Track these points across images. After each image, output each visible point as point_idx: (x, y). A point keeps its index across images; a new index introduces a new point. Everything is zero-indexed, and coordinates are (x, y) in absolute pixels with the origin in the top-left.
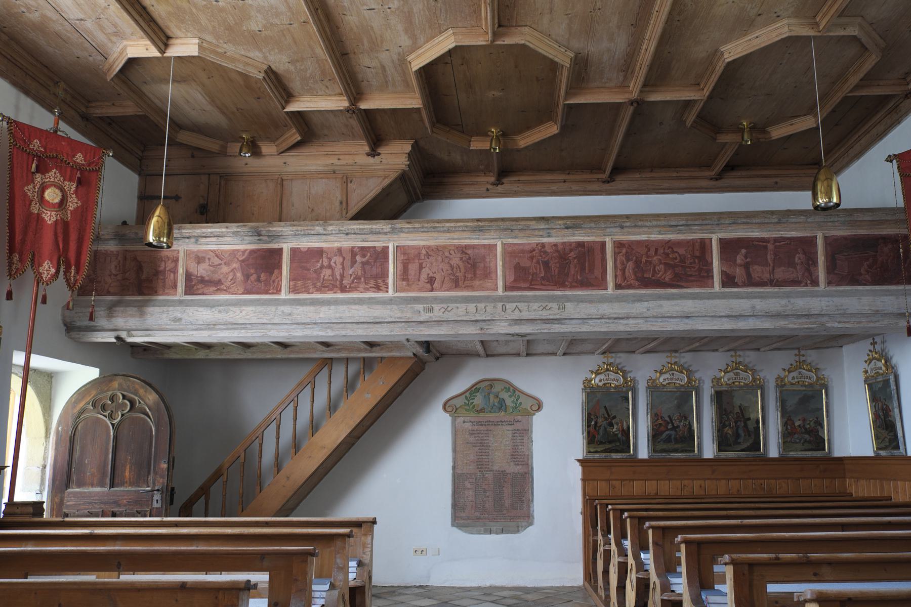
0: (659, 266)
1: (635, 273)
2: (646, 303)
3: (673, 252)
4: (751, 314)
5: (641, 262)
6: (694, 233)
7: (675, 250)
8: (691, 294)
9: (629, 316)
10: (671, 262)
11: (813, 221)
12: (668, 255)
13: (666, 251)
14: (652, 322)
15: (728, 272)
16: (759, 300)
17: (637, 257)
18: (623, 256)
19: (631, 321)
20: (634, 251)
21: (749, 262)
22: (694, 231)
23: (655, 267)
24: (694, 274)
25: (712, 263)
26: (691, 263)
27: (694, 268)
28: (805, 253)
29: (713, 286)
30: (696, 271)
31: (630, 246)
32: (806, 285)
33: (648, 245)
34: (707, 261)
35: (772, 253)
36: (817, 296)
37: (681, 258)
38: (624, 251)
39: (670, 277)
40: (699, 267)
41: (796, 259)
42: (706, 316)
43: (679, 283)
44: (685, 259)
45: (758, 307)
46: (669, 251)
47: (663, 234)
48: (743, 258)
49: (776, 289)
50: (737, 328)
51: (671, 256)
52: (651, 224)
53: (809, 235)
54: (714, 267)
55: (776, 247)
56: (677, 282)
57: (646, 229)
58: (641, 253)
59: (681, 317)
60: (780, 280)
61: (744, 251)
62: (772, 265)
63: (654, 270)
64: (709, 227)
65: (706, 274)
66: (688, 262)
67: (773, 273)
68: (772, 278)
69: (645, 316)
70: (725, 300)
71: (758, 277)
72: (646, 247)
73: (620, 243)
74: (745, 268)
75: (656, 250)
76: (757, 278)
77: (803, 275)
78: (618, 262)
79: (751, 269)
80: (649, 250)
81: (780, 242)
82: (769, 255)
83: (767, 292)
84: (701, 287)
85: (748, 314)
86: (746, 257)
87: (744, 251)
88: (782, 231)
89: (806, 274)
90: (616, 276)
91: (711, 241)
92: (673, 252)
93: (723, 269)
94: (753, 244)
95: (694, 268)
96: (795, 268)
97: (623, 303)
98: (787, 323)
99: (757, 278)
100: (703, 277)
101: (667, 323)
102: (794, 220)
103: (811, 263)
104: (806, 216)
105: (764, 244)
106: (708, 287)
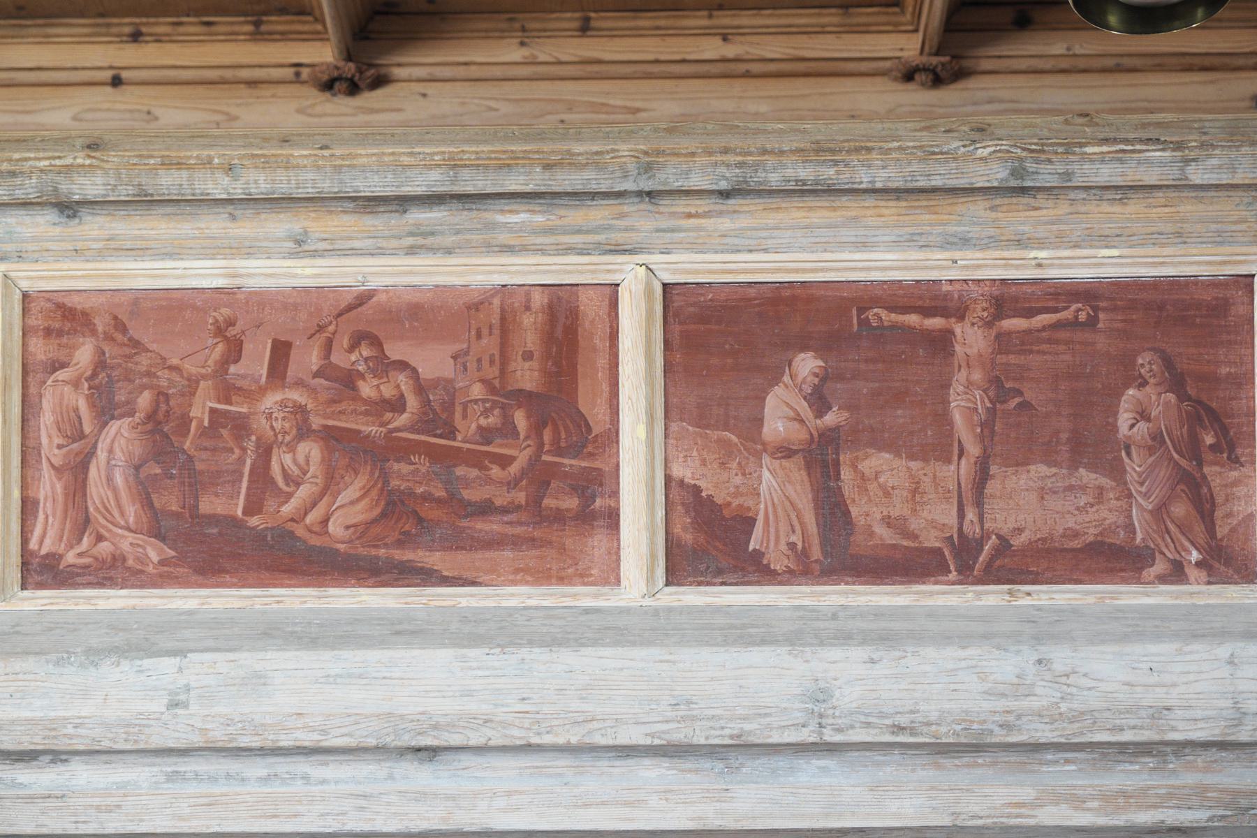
0: (292, 450)
1: (144, 493)
3: (383, 366)
4: (807, 735)
5: (185, 422)
6: (508, 249)
7: (395, 351)
8: (467, 617)
9: (62, 744)
10: (371, 429)
11: (1225, 179)
12: (348, 380)
14: (213, 779)
15: (707, 487)
16: (858, 653)
17: (162, 395)
19: (81, 775)
20: (144, 361)
21: (837, 429)
22: (503, 238)
23: (265, 452)
24: (498, 502)
25: (612, 436)
26: (486, 435)
27: (504, 461)
28: (1176, 381)
29: (612, 577)
30: (513, 484)
31: (120, 326)
32: (1177, 574)
33: (231, 323)
34: (583, 424)
35: (977, 376)
36: (1223, 635)
37: (426, 403)
38: (84, 355)
39: (359, 514)
40: (535, 460)
41: (1124, 420)
42: (528, 748)
43: (408, 555)
44: (449, 406)
45: (848, 697)
46: (356, 359)
47: (315, 254)
48: (804, 408)
49: (992, 597)
50: (731, 824)
51: (367, 389)
52: (238, 190)
53: (1204, 271)
55: (1003, 342)
56: (400, 544)
57: (215, 225)
58: (190, 367)
59: (380, 751)
60: (1017, 542)
61: (807, 365)
62: (973, 450)
63: (261, 475)
64: (598, 214)
65: (571, 503)
66: (467, 427)
67: (979, 504)
68: (972, 527)
69: (156, 742)
70: (655, 652)
71: (888, 521)
72: (219, 331)
73: (60, 306)
74: (809, 466)
75: (281, 351)
76: (881, 531)
77: (1160, 512)
78: (47, 419)
79: (846, 474)
80: (235, 350)
81: (1030, 313)
82: (957, 387)
83: (932, 614)
84: (542, 576)
85: (790, 737)
86: (819, 402)
87: (807, 365)
88: (1041, 244)
89: (1180, 509)
90: (28, 507)
92: (383, 366)
93: (678, 471)
94: (864, 323)
95: (504, 461)
96: (1117, 471)
98: (1026, 793)
99: (881, 531)
100: (559, 517)
101: (298, 787)
102: (1106, 174)
103: (1209, 440)
104: (1179, 146)
105: (936, 323)
106: (583, 577)
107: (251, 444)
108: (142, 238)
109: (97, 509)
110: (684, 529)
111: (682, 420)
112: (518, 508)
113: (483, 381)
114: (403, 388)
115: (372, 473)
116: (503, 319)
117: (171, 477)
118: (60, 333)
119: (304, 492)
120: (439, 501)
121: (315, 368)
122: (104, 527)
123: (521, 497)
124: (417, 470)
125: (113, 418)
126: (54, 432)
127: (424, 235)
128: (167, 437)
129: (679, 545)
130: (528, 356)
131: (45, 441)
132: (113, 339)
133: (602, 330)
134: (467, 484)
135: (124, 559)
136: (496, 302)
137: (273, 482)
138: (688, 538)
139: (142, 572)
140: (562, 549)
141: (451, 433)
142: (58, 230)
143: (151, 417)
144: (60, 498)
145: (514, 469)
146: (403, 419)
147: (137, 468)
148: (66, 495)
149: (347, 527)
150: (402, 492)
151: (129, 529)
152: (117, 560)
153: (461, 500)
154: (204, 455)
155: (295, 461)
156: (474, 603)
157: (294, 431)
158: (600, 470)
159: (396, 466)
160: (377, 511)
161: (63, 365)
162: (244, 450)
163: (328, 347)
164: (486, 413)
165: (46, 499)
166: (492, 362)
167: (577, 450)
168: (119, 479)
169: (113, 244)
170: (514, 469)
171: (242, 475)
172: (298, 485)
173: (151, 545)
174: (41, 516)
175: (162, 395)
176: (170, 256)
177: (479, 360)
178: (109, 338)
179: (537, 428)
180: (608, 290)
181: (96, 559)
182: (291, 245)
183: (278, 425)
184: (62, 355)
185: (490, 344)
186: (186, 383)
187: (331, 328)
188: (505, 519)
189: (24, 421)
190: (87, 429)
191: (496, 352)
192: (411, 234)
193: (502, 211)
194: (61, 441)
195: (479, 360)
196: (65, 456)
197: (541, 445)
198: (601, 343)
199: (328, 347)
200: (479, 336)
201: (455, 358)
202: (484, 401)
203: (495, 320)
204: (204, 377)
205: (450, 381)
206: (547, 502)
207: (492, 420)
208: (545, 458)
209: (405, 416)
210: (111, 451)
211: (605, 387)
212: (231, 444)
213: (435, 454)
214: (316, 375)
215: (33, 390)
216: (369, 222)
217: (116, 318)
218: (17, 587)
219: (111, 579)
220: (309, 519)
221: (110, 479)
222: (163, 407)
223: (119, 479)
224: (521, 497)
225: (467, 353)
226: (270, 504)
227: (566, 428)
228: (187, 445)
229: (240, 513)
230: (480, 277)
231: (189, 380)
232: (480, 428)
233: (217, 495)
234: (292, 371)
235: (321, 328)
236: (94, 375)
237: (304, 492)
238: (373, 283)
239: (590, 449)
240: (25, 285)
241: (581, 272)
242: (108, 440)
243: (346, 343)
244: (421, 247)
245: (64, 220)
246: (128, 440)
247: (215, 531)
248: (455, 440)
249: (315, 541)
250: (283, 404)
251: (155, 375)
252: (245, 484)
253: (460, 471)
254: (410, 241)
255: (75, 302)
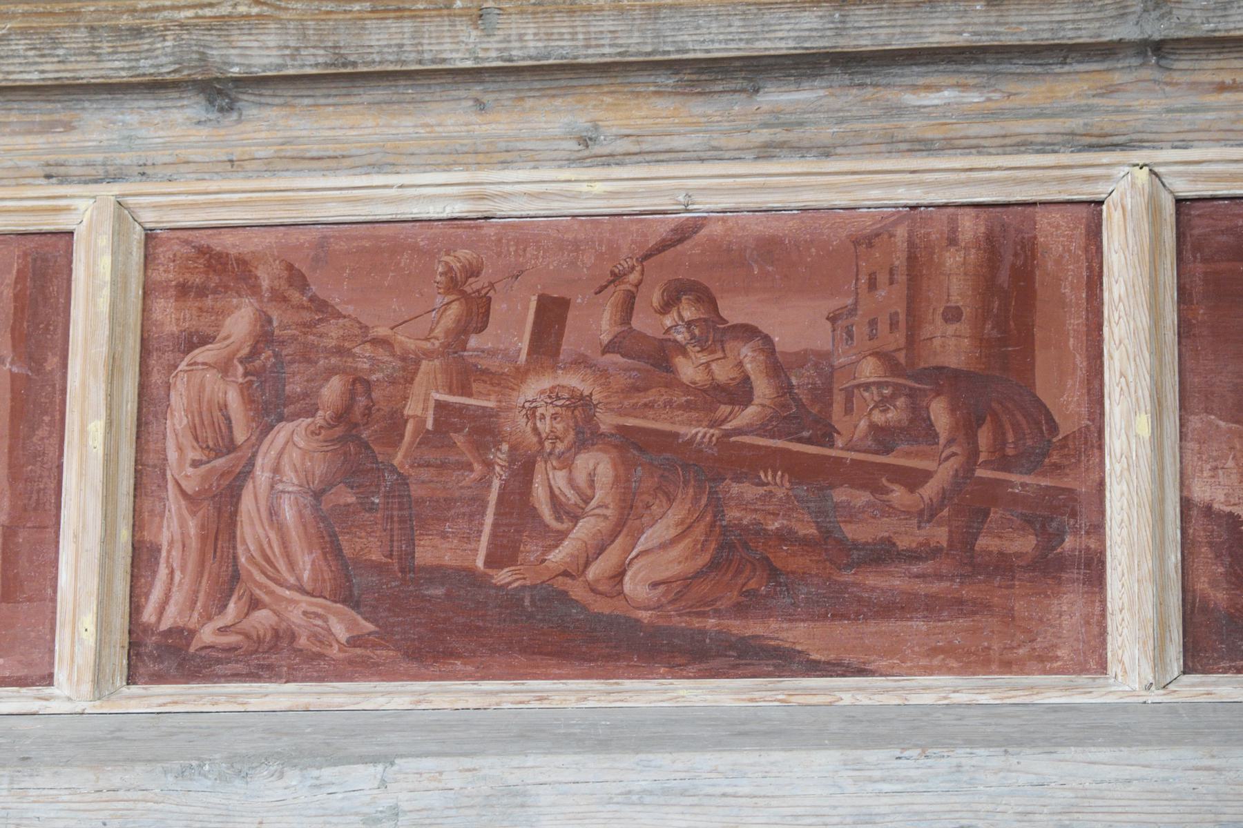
0: (566, 463)
2: (364, 776)
5: (396, 424)
6: (923, 146)
7: (734, 310)
8: (851, 716)
10: (696, 431)
13: (639, 323)
17: (359, 383)
18: (224, 368)
20: (333, 332)
23: (524, 469)
24: (903, 543)
26: (884, 438)
27: (913, 479)
30: (928, 514)
31: (296, 278)
33: (473, 271)
34: (1044, 420)
37: (786, 390)
39: (673, 564)
43: (754, 628)
44: (823, 394)
51: (688, 370)
54: (1114, 466)
56: (740, 610)
58: (406, 340)
72: (454, 284)
73: (204, 251)
78: (177, 420)
91: (1094, 232)
93: (1201, 492)
95: (913, 479)
97: (137, 775)
100: (1003, 566)
106: (1044, 661)
107: (500, 456)
108: (336, 140)
109: (251, 559)
110: (1214, 584)
111: (1208, 411)
112: (935, 552)
113: (875, 354)
114: (748, 366)
115: (696, 500)
116: (912, 259)
117: (372, 508)
118: (202, 292)
119: (584, 530)
120: (805, 542)
121: (605, 338)
122: (260, 586)
123: (940, 535)
124: (771, 495)
125: (281, 418)
126: (188, 441)
127: (788, 126)
128: (367, 447)
129: (1205, 610)
130: (952, 315)
131: (172, 455)
132: (285, 299)
133: (1075, 271)
134: (852, 515)
135: (293, 637)
136: (901, 232)
137: (535, 514)
138: (1220, 597)
139: (321, 656)
140: (1009, 617)
141: (826, 435)
142: (204, 132)
143: (342, 416)
144: (194, 544)
145: (929, 491)
146: (749, 414)
147: (318, 495)
148: (203, 539)
149: (655, 585)
150: (745, 529)
151: (301, 590)
152: (281, 638)
153: (841, 542)
154: (425, 474)
155: (571, 482)
156: (863, 699)
157: (571, 436)
158: (1071, 491)
159: (735, 488)
160: (703, 559)
161: (205, 340)
162: (489, 465)
163: (628, 306)
164: (884, 404)
165: (171, 543)
166: (893, 325)
167: (1034, 461)
168: (288, 513)
169: (290, 150)
170: (929, 491)
171: (484, 506)
172: (575, 519)
173: (337, 614)
174: (163, 571)
175: (359, 383)
176: (377, 167)
177: (873, 323)
178: (279, 298)
179: (968, 426)
180: (1083, 211)
181: (247, 636)
182: (573, 145)
183: (544, 427)
184: (210, 331)
185: (890, 297)
186: (399, 364)
187: (634, 277)
188: (915, 569)
189: (141, 424)
190: (240, 436)
191: (901, 310)
192: (766, 125)
193: (914, 88)
194: (197, 455)
195: (873, 323)
196: (204, 478)
197: (975, 453)
198: (1073, 293)
199: (628, 306)
200: (873, 285)
201: (833, 319)
202: (879, 385)
203: (899, 260)
204: (428, 355)
205: (826, 355)
206: (982, 542)
207: (894, 415)
208: (980, 473)
209: (751, 410)
210: (276, 470)
211: (1081, 362)
212: (469, 457)
213: (798, 469)
214: (607, 349)
215: (156, 378)
216: (699, 108)
217: (290, 267)
218: (120, 680)
219: (270, 667)
220: (592, 573)
221: (273, 513)
222: (362, 401)
223: (288, 513)
224: (940, 535)
225: (853, 311)
226: (531, 550)
227: (1016, 427)
228: (398, 459)
229: (480, 563)
230: (875, 194)
231: (403, 359)
232: (873, 427)
233: (444, 536)
234: (570, 344)
235: (616, 277)
236: (254, 353)
237: (584, 530)
238: (705, 204)
239: (1055, 458)
240: (149, 218)
241: (1041, 182)
242: (273, 453)
243: (656, 298)
244: (781, 145)
245: (212, 116)
246: (305, 452)
247: (439, 591)
248: (832, 445)
249: (601, 606)
250: (553, 394)
251: (350, 353)
252: (489, 519)
253: (840, 495)
254: (765, 135)
255: (228, 243)
